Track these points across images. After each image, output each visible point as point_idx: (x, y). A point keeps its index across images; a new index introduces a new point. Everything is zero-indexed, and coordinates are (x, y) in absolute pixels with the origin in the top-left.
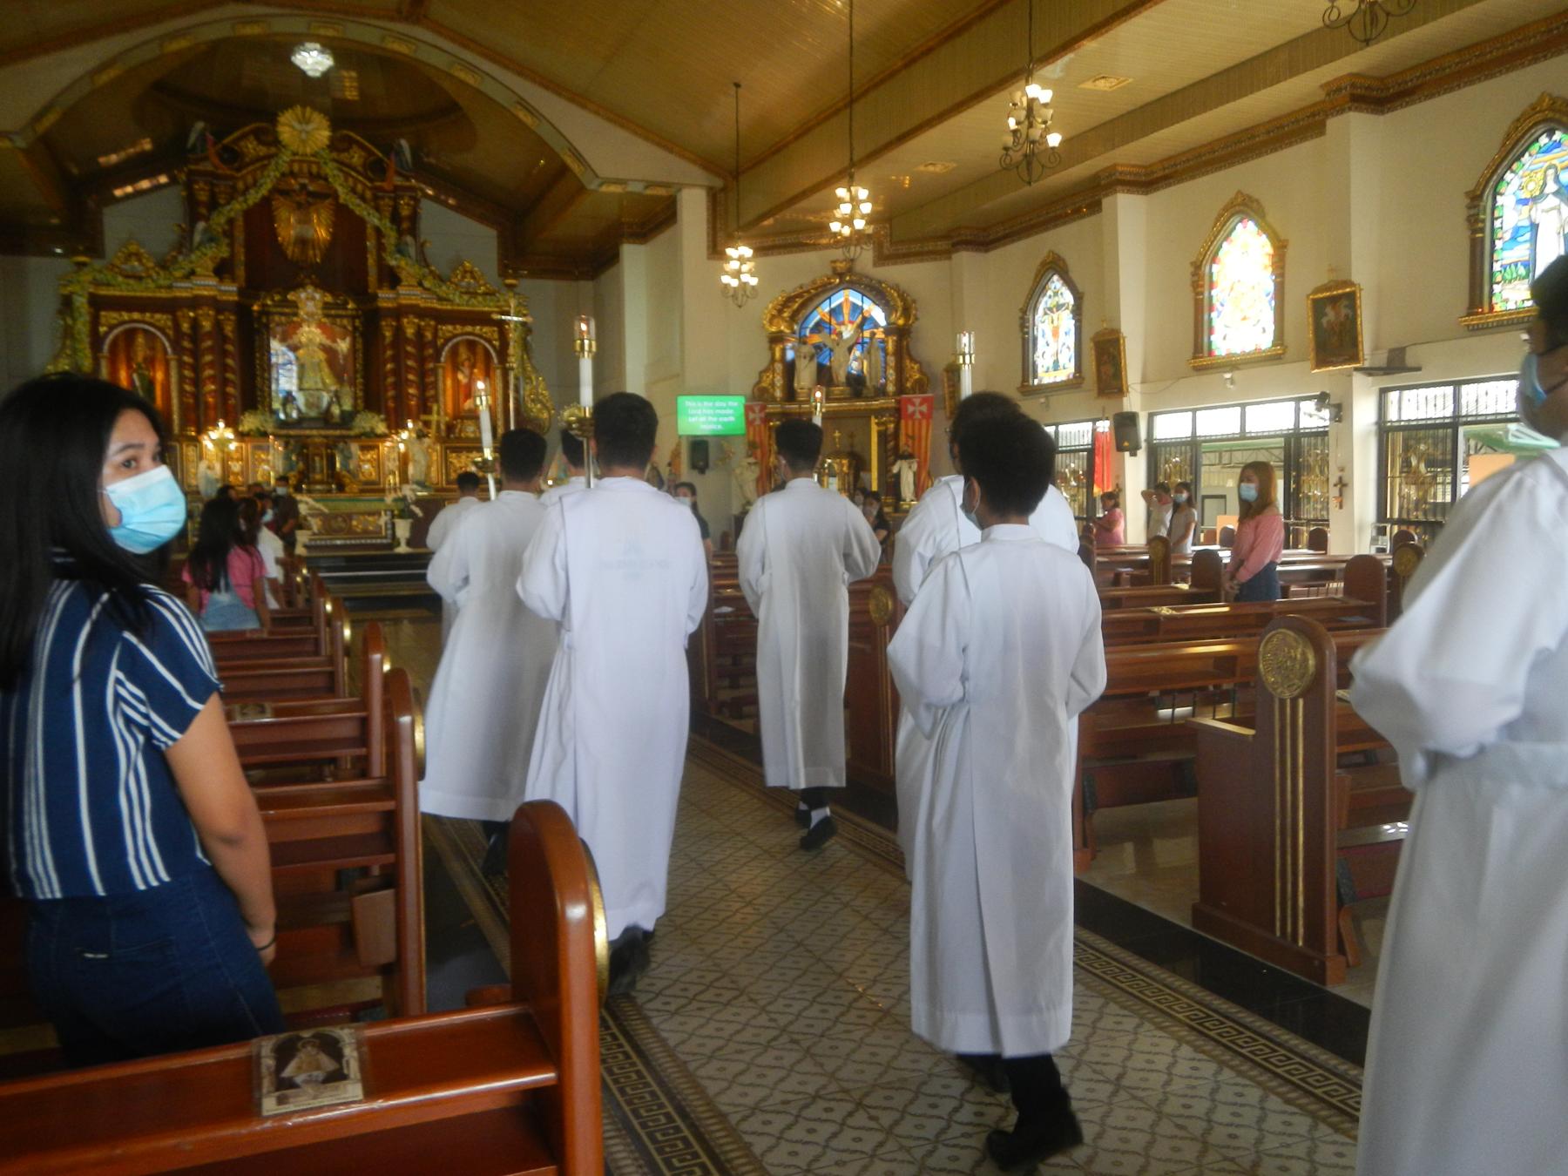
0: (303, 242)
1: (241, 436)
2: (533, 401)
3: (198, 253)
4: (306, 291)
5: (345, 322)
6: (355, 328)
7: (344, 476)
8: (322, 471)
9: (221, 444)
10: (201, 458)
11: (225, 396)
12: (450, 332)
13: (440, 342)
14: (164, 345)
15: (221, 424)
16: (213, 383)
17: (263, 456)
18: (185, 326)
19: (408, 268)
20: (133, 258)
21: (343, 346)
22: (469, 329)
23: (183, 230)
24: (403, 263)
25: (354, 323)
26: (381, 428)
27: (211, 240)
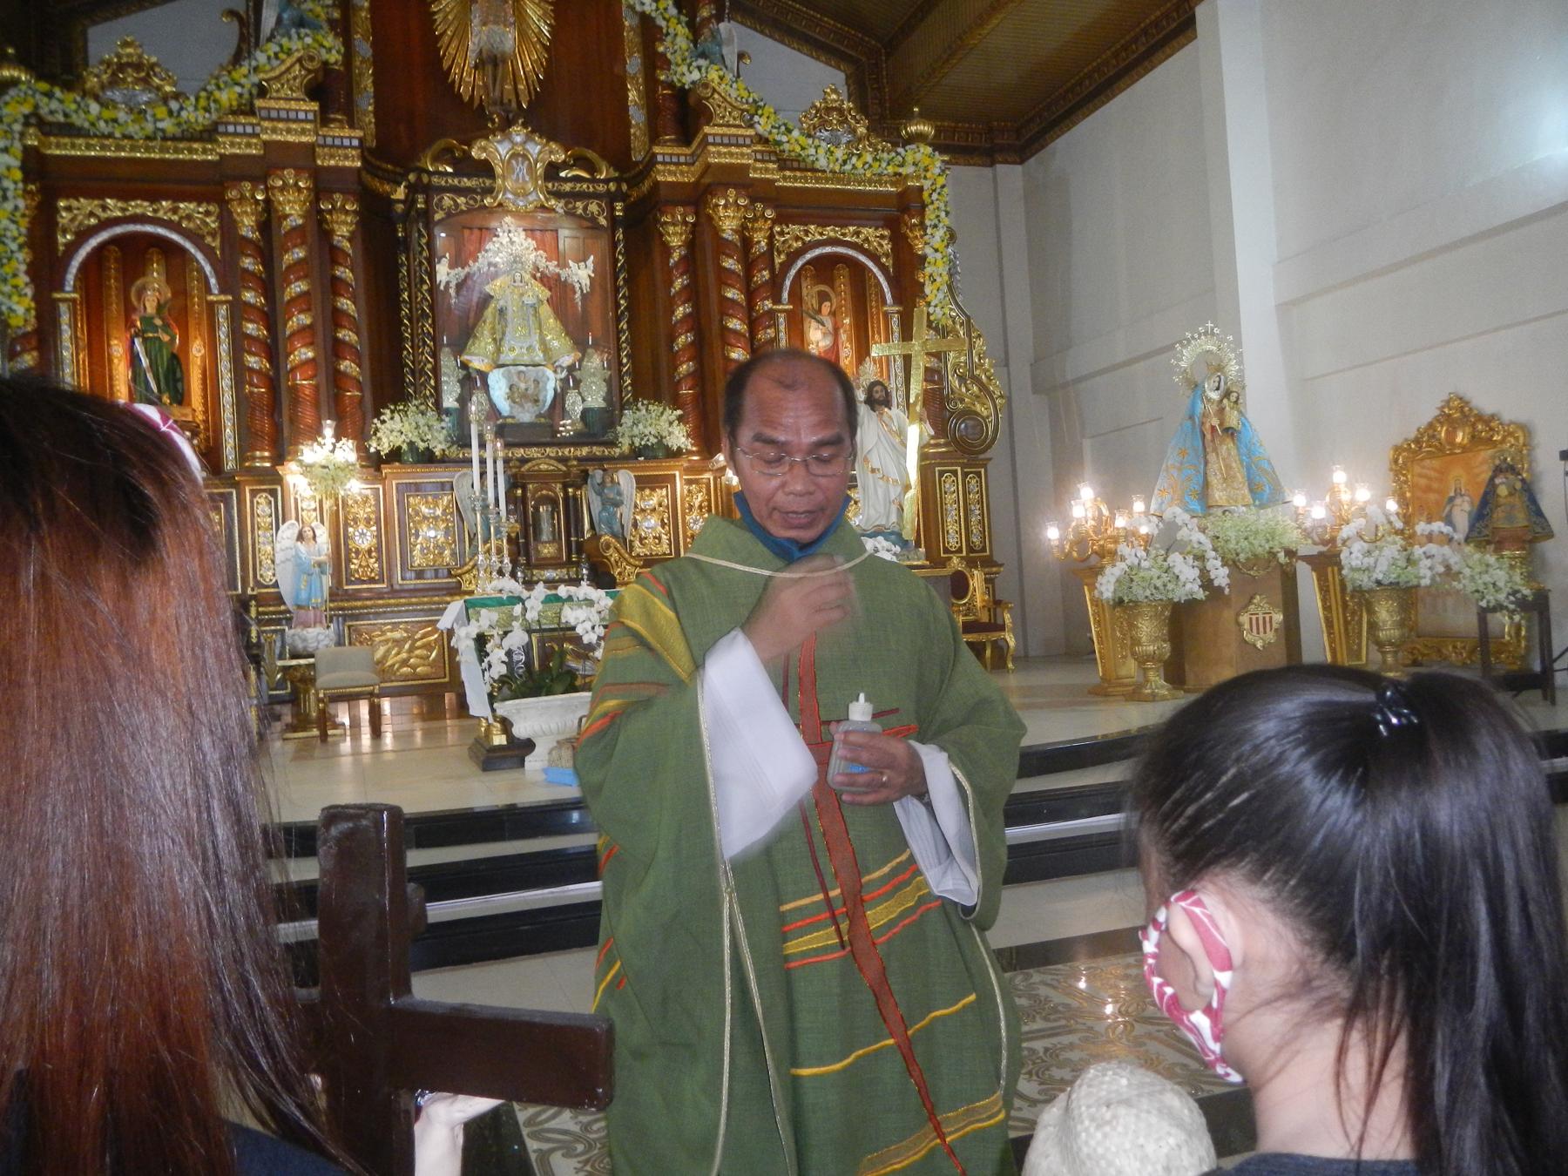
0: (491, 62)
1: (375, 463)
2: (962, 378)
3: (272, 48)
4: (508, 137)
5: (593, 207)
6: (613, 219)
7: (608, 546)
8: (555, 538)
9: (329, 476)
10: (280, 518)
11: (337, 380)
12: (797, 238)
13: (779, 260)
14: (201, 270)
15: (329, 431)
16: (310, 344)
17: (425, 510)
18: (247, 225)
19: (720, 89)
20: (130, 76)
21: (581, 274)
22: (830, 232)
23: (243, 23)
24: (714, 75)
25: (613, 209)
26: (679, 437)
27: (301, 23)
